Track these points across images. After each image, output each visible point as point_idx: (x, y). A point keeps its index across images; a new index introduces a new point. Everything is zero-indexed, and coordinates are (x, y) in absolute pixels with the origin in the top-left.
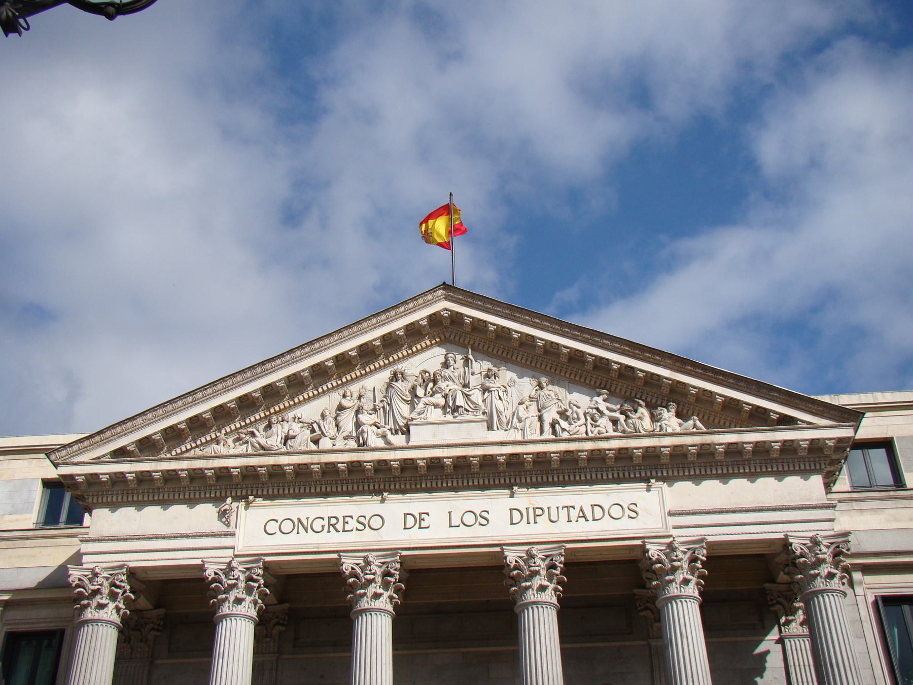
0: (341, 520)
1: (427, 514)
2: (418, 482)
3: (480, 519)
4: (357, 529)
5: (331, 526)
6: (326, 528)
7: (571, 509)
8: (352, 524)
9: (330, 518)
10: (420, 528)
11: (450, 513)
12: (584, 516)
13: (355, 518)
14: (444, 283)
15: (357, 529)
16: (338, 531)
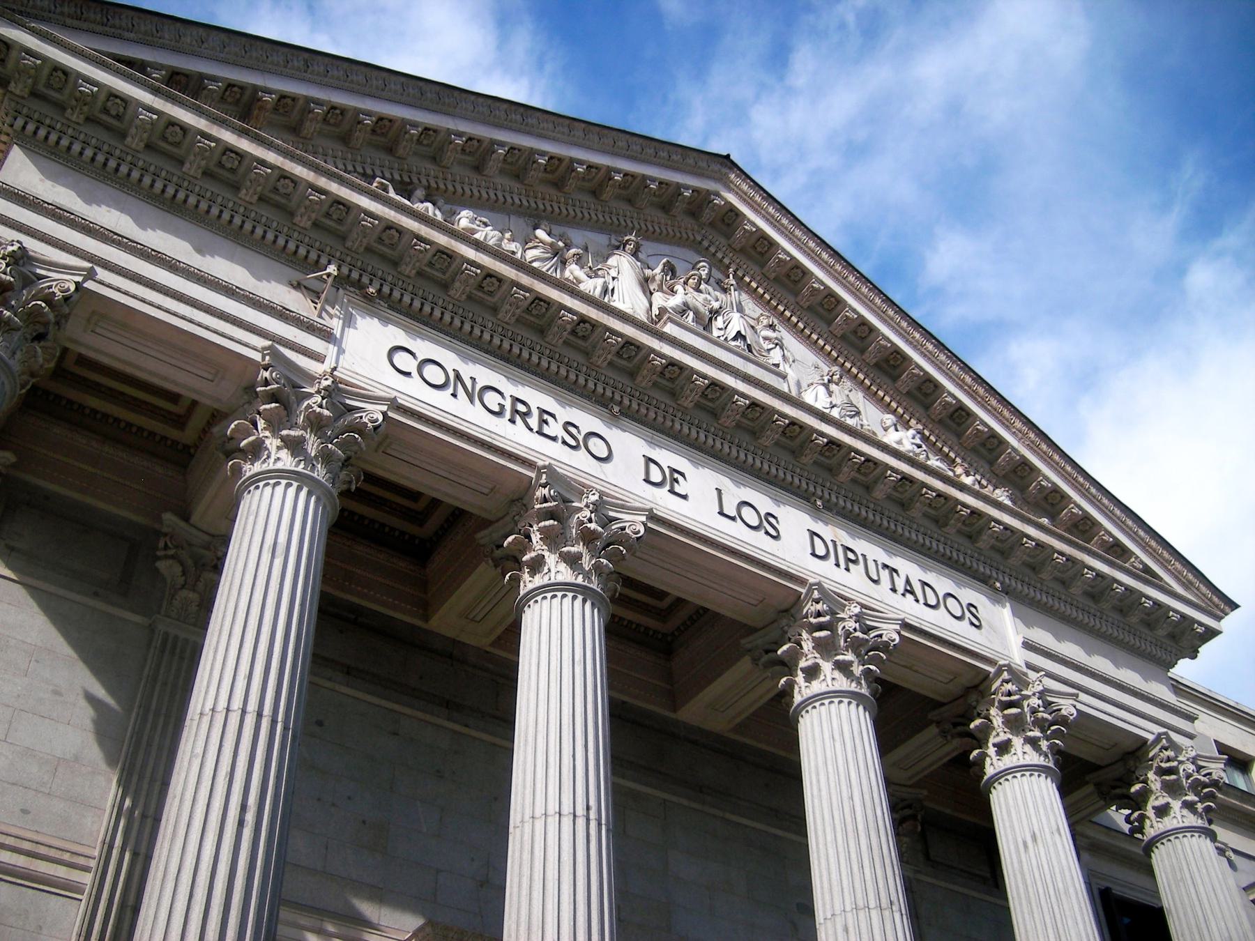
0: (535, 413)
1: (682, 474)
2: (669, 417)
3: (765, 524)
4: (564, 442)
5: (518, 418)
6: (508, 415)
7: (895, 574)
8: (554, 428)
9: (516, 400)
10: (672, 491)
11: (719, 491)
12: (912, 593)
13: (561, 422)
14: (728, 156)
15: (564, 442)
16: (531, 430)
